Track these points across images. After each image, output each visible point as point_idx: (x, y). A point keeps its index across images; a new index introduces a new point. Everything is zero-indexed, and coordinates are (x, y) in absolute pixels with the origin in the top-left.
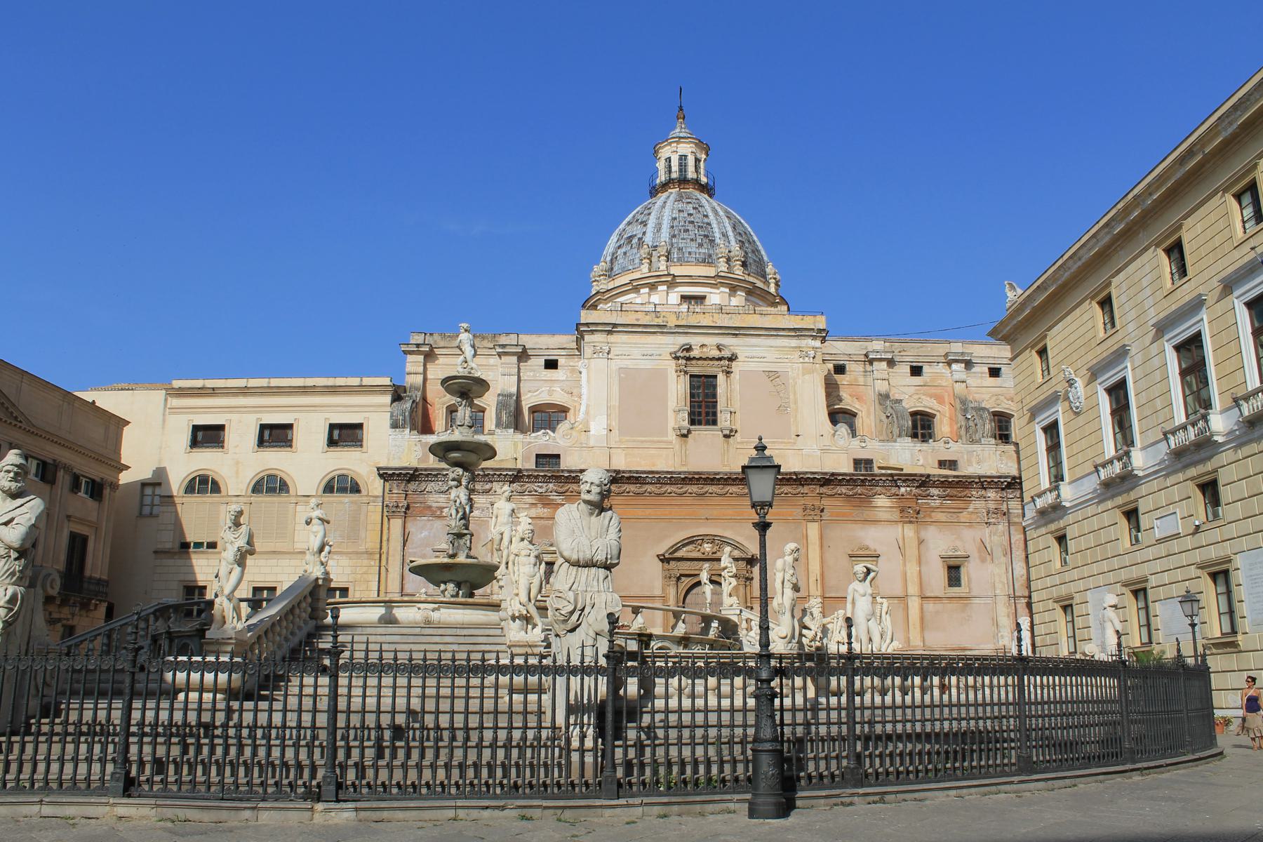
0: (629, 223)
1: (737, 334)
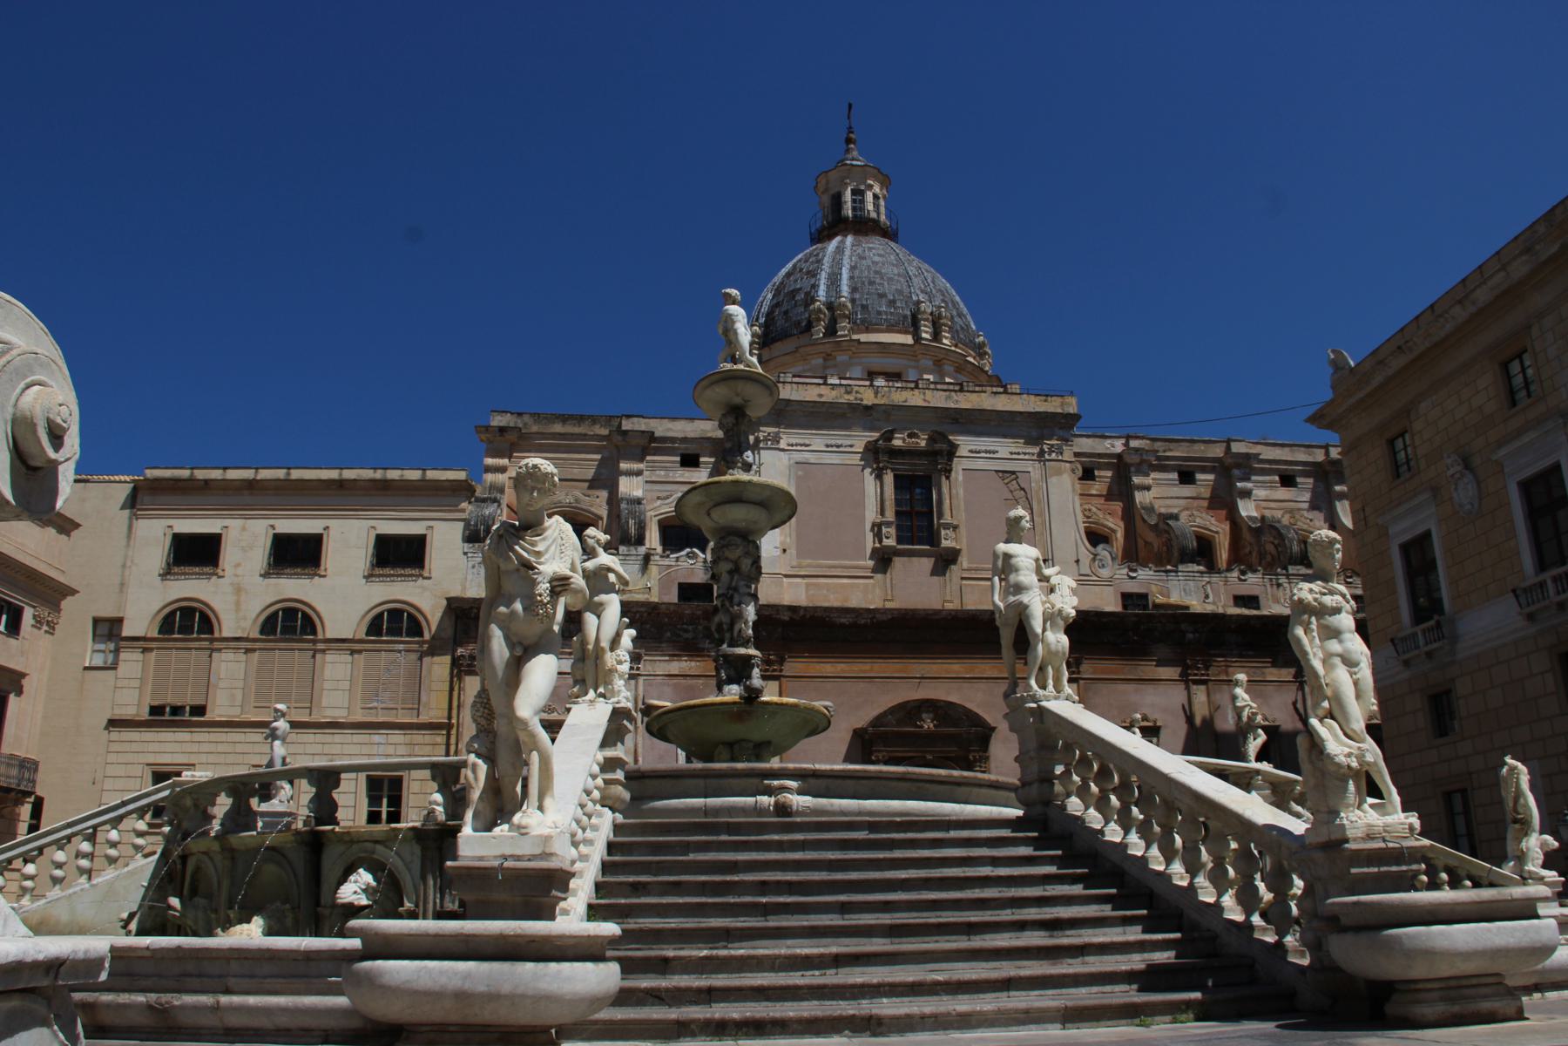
0: (788, 275)
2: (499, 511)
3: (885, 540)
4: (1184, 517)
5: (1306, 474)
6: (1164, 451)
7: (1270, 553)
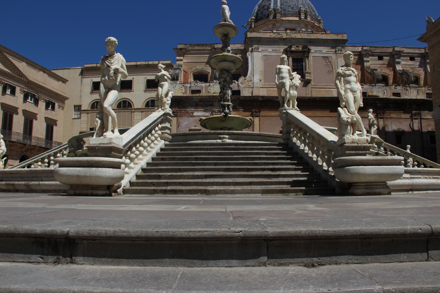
2: (180, 72)
4: (379, 70)
5: (418, 57)
6: (374, 50)
7: (405, 81)
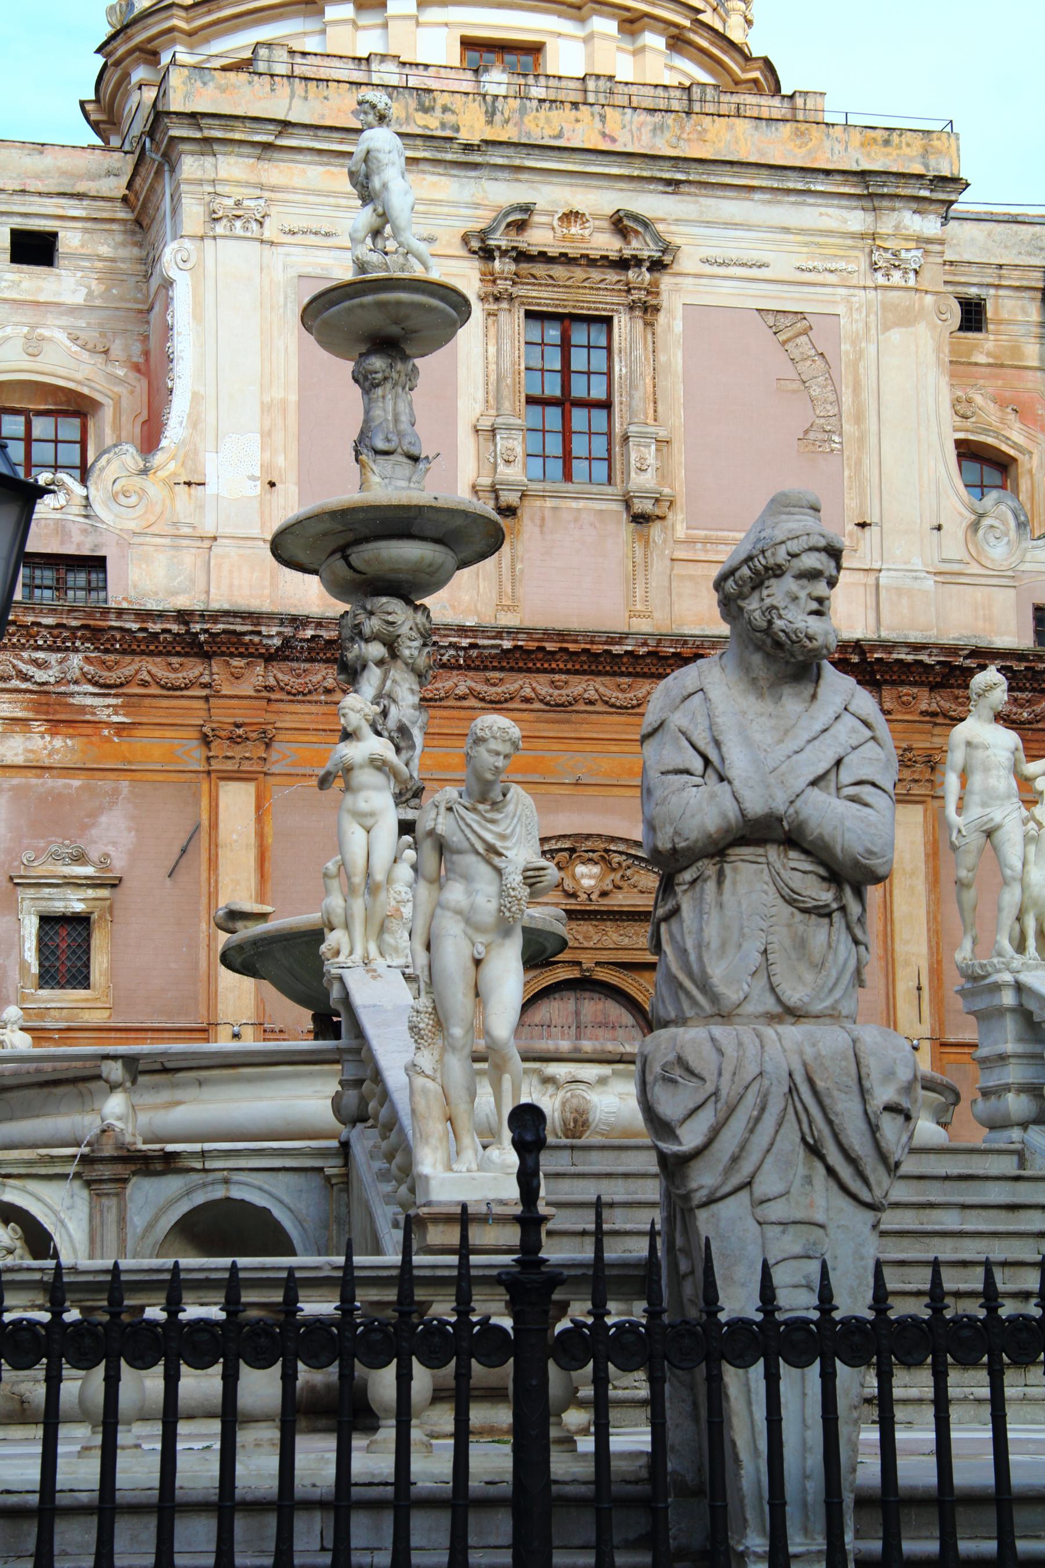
1: (678, 183)
3: (501, 467)
